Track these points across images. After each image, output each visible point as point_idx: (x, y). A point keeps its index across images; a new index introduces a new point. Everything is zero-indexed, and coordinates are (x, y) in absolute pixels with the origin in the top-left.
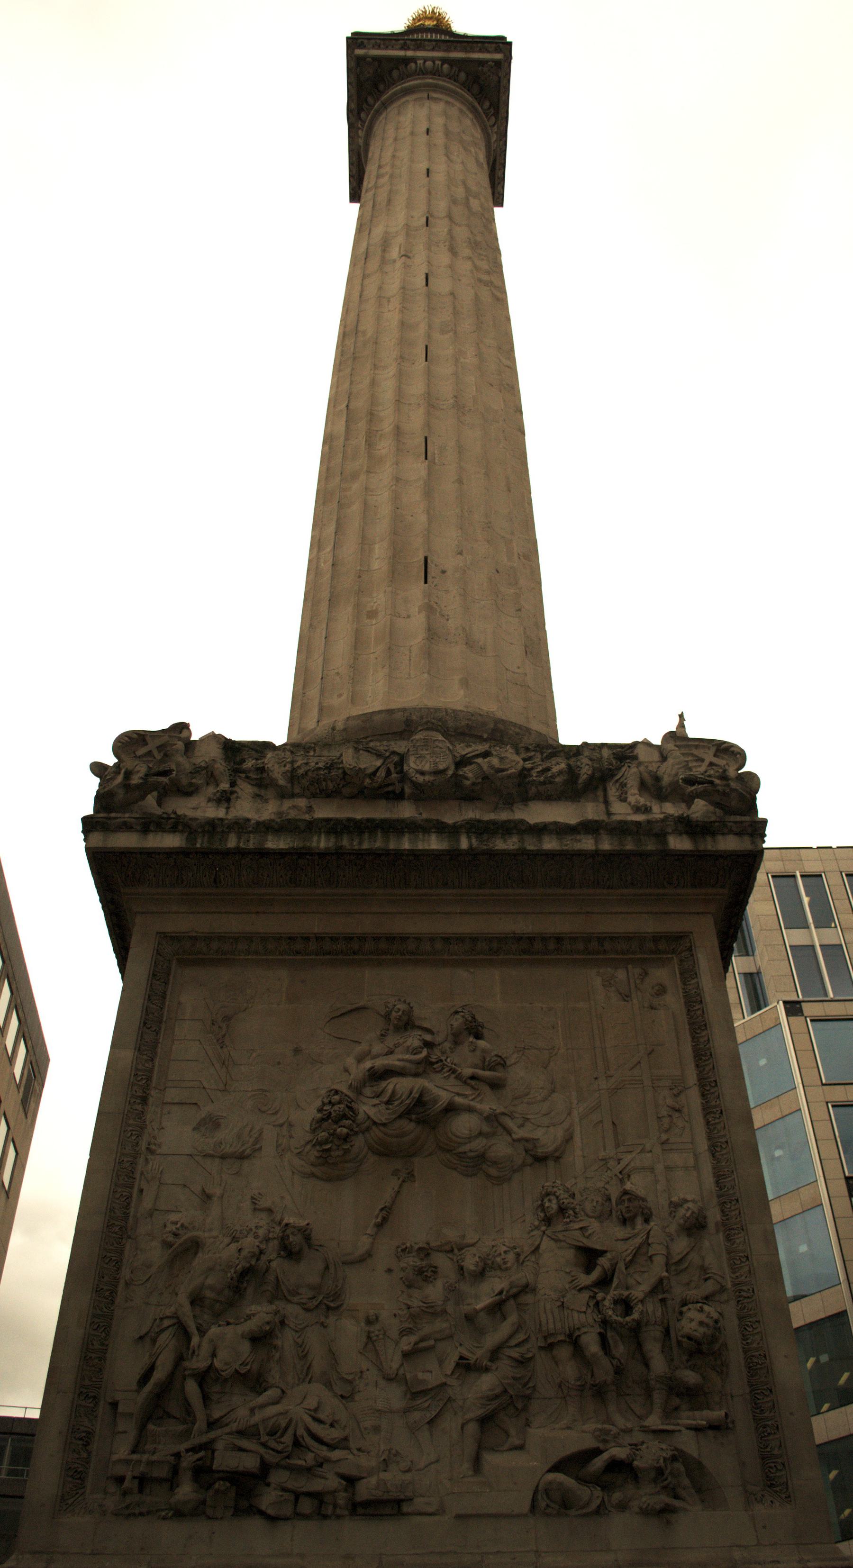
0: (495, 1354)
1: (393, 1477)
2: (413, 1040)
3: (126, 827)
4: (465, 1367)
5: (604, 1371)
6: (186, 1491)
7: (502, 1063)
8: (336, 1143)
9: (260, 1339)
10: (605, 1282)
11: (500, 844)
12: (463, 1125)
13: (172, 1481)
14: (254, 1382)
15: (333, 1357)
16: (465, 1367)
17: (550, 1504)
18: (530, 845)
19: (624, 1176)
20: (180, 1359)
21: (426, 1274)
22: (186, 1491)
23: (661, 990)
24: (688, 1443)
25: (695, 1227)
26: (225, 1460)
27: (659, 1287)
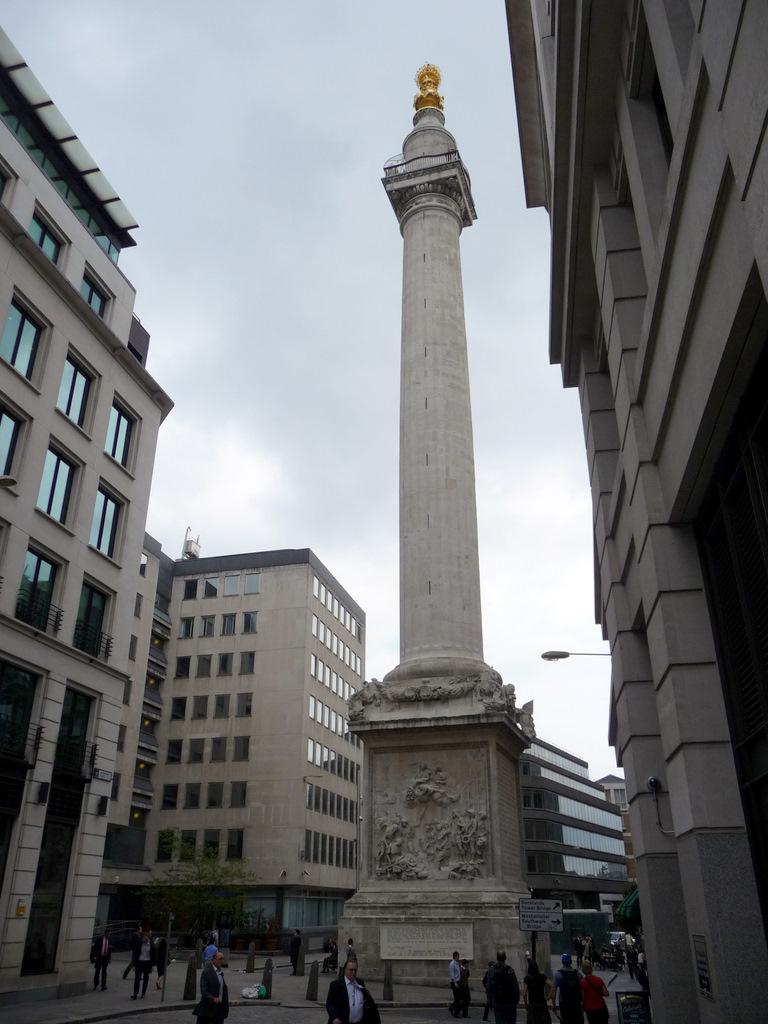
0: (443, 847)
1: (424, 872)
2: (426, 773)
3: (356, 725)
4: (438, 850)
5: (463, 852)
6: (389, 875)
7: (446, 779)
8: (411, 802)
9: (399, 846)
10: (463, 833)
11: (441, 724)
12: (437, 796)
13: (387, 873)
14: (399, 854)
15: (413, 847)
16: (438, 850)
17: (452, 877)
18: (449, 723)
19: (471, 806)
20: (385, 850)
21: (430, 829)
22: (389, 875)
23: (483, 755)
24: (477, 866)
25: (484, 819)
26: (394, 870)
27: (474, 834)
